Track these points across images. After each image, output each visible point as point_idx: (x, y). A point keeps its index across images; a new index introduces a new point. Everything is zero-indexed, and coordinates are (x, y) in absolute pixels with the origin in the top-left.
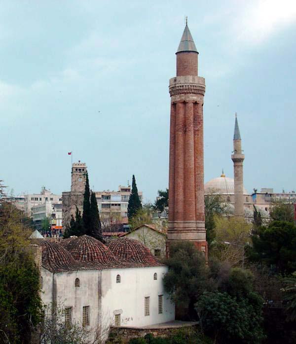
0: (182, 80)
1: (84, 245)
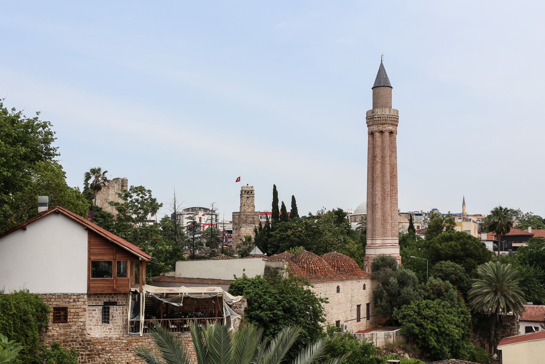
0: (379, 112)
1: (307, 260)
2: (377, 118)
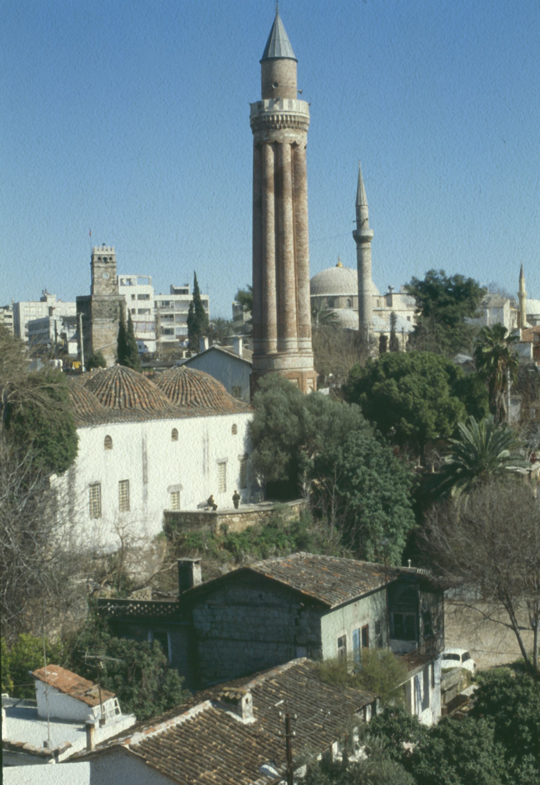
1: (118, 382)
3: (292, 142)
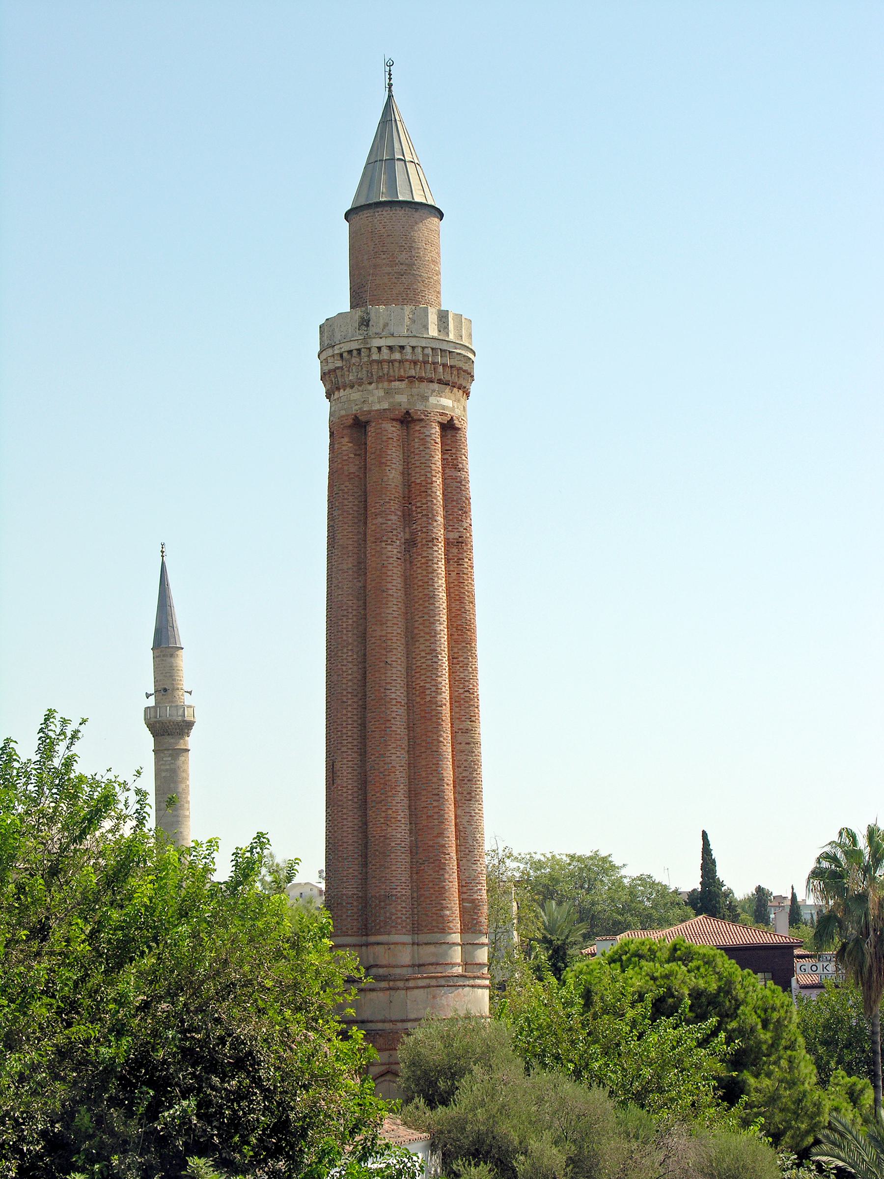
2: (385, 351)
3: (445, 420)
